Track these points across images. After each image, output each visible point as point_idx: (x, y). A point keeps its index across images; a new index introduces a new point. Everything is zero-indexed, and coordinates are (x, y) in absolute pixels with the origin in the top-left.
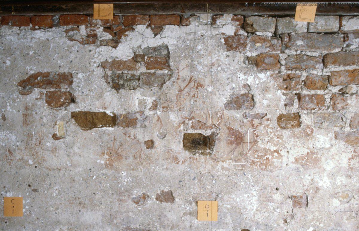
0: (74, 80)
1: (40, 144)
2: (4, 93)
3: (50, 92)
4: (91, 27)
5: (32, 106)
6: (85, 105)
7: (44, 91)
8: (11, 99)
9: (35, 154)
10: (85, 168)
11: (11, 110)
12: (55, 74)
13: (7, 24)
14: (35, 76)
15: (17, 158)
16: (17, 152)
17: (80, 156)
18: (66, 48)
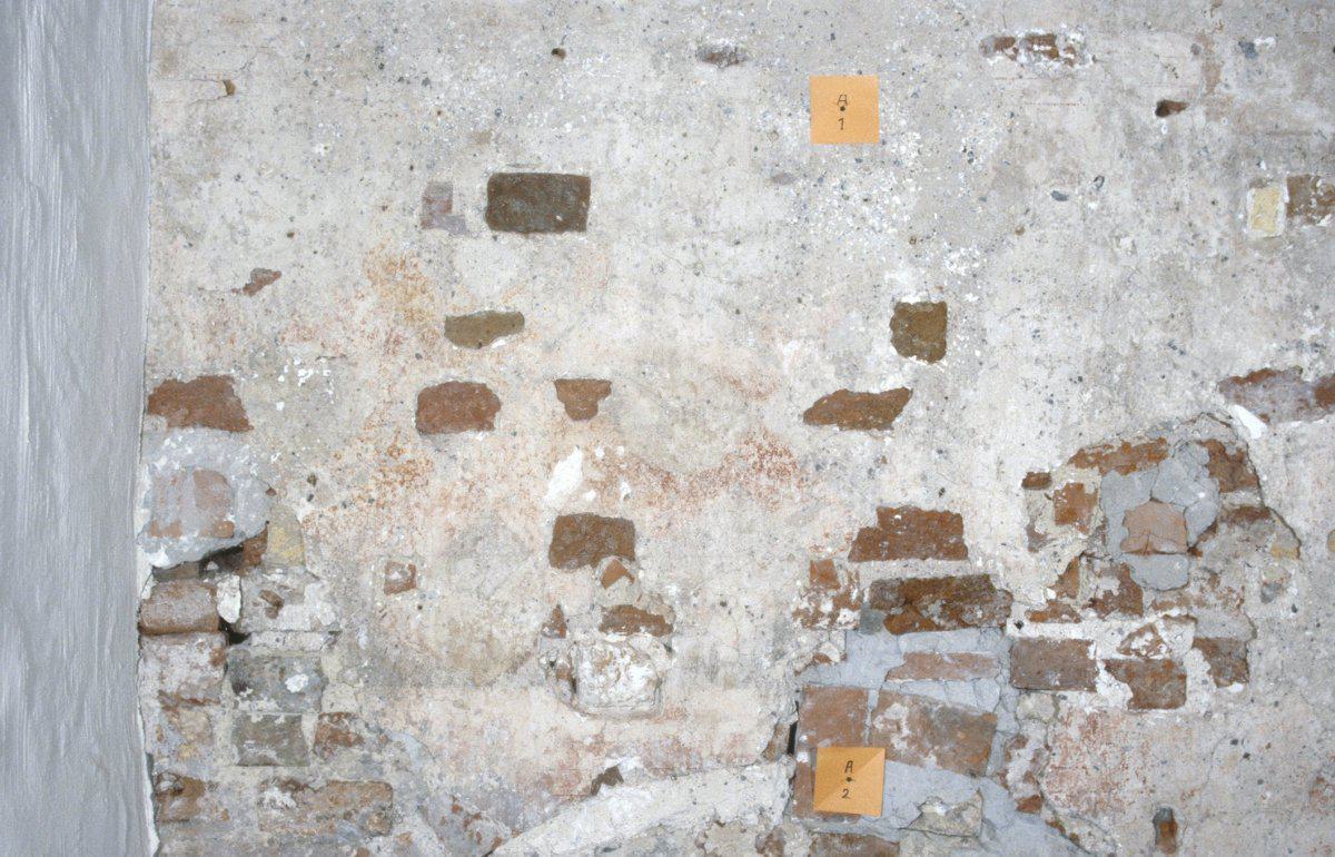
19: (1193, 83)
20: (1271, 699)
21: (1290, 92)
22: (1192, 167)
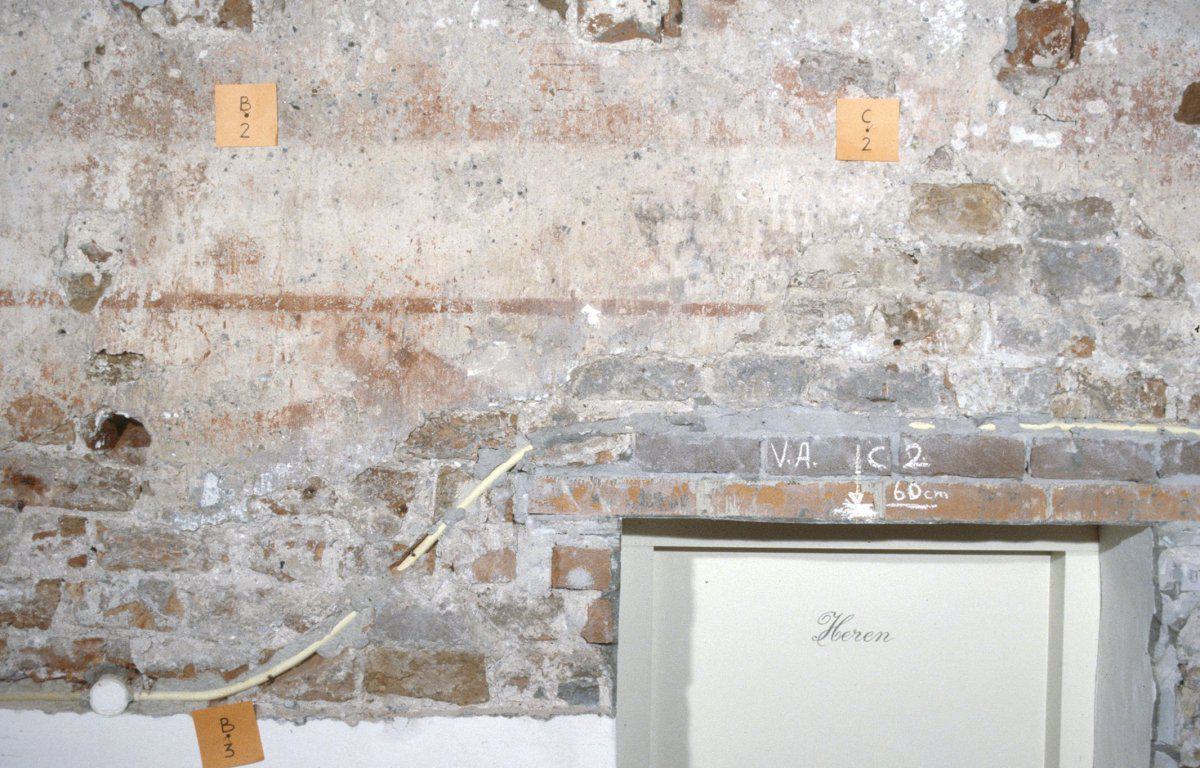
20: (15, 30)
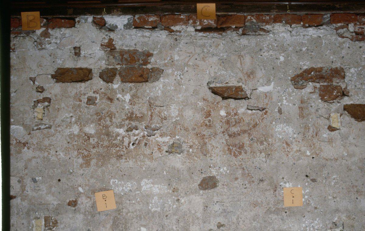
0: (347, 74)
1: (316, 135)
2: (279, 88)
3: (323, 86)
4: (360, 25)
5: (307, 100)
6: (358, 98)
7: (318, 85)
8: (287, 93)
9: (312, 145)
10: (361, 157)
11: (287, 104)
12: (328, 69)
13: (281, 22)
14: (308, 71)
15: (295, 150)
16: (294, 144)
17: (356, 145)
18: (338, 45)
19: (18, 190)
21: (45, 193)
22: (17, 214)
